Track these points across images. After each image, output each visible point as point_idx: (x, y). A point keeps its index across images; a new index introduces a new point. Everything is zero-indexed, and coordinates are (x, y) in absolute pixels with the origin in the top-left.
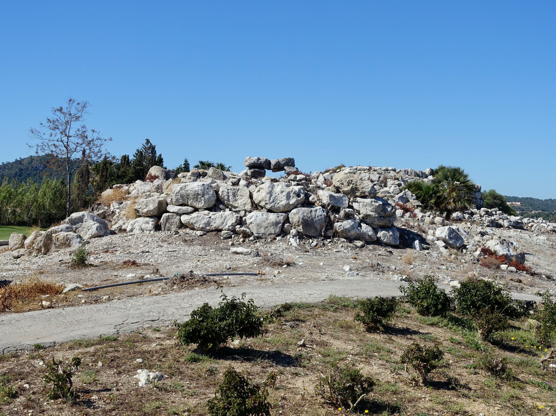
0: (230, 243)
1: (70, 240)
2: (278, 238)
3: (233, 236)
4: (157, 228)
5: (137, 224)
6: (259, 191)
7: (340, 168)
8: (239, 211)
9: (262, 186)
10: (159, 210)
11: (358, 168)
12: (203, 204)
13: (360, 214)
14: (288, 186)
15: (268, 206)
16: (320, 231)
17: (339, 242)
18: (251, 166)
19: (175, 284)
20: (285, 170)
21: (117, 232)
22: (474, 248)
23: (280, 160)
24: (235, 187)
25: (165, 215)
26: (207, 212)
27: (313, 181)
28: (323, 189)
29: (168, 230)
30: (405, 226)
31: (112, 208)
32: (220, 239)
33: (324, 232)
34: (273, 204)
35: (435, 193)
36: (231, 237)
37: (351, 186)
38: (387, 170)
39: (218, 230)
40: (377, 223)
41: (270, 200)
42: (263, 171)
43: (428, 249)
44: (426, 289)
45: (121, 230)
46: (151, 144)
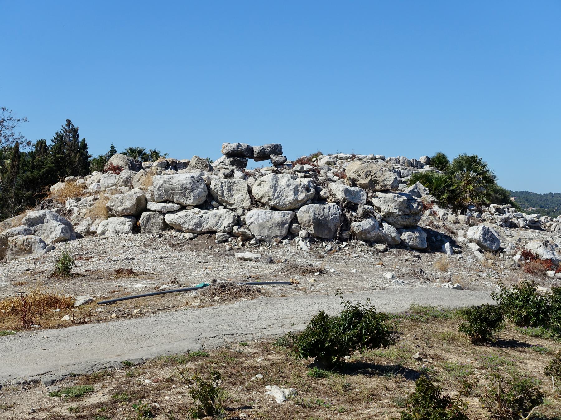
0: (228, 248)
1: (31, 245)
2: (285, 241)
3: (230, 239)
4: (136, 229)
5: (110, 225)
6: (260, 184)
8: (236, 209)
9: (263, 178)
10: (137, 208)
11: (339, 157)
12: (192, 201)
13: (380, 212)
14: (294, 178)
15: (272, 203)
16: (333, 232)
17: (357, 246)
18: (229, 155)
19: (215, 294)
20: (271, 159)
21: (83, 235)
22: (512, 251)
23: (266, 146)
24: (230, 180)
25: (145, 214)
26: (197, 210)
27: (322, 172)
28: (335, 182)
29: (150, 232)
30: (429, 225)
31: (68, 207)
32: (214, 243)
33: (339, 233)
34: (278, 200)
35: (449, 185)
36: (227, 241)
37: (370, 178)
38: (375, 158)
39: (212, 232)
40: (401, 222)
41: (274, 195)
42: (244, 160)
43: (460, 253)
44: (524, 296)
45: (89, 233)
46: (73, 126)
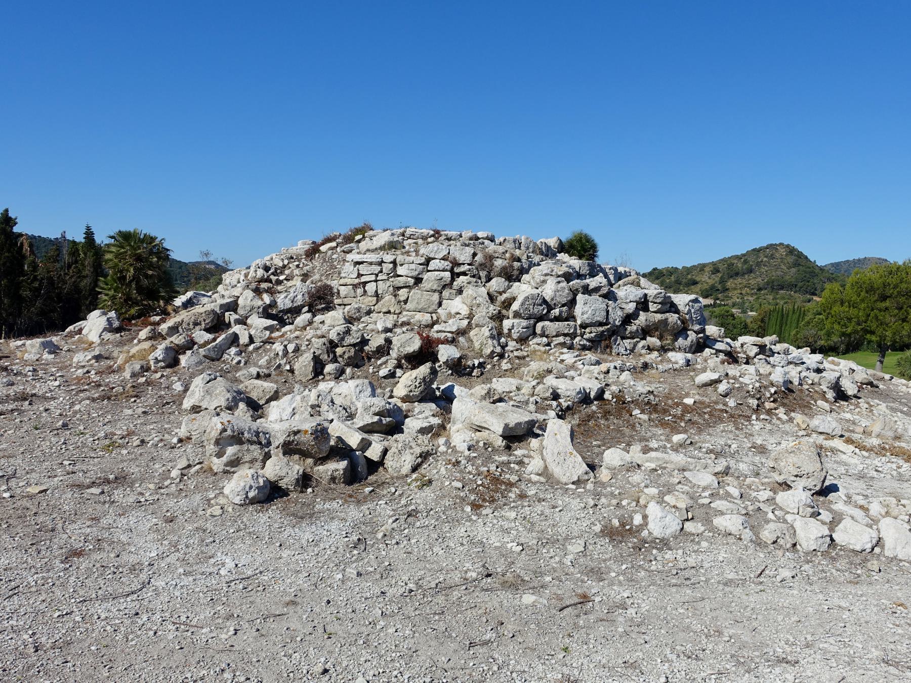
7: (362, 231)
11: (408, 233)
38: (477, 239)
